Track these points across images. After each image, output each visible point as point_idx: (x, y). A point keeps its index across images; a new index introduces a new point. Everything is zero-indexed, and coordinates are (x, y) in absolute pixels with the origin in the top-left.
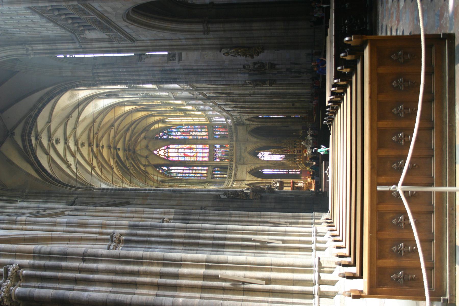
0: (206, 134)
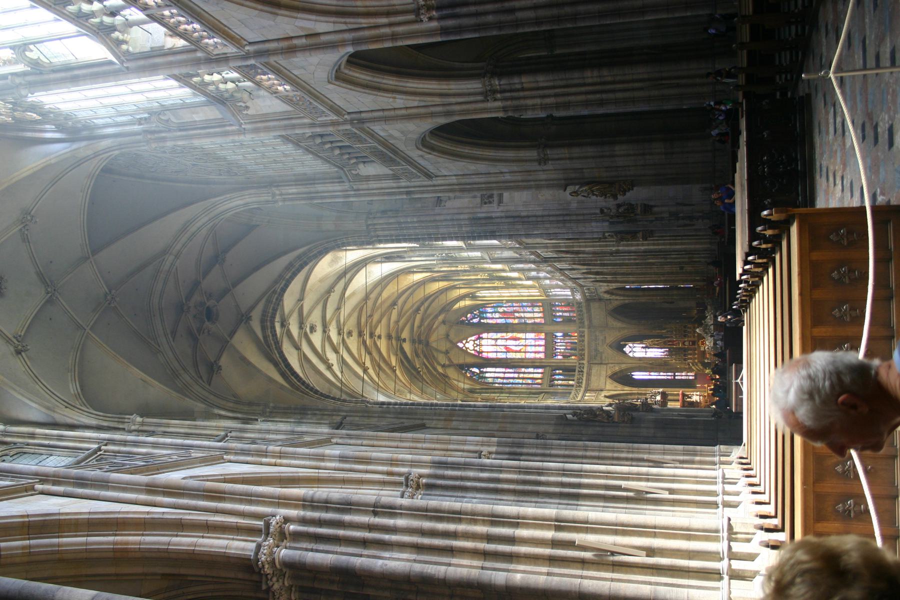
0: (541, 315)
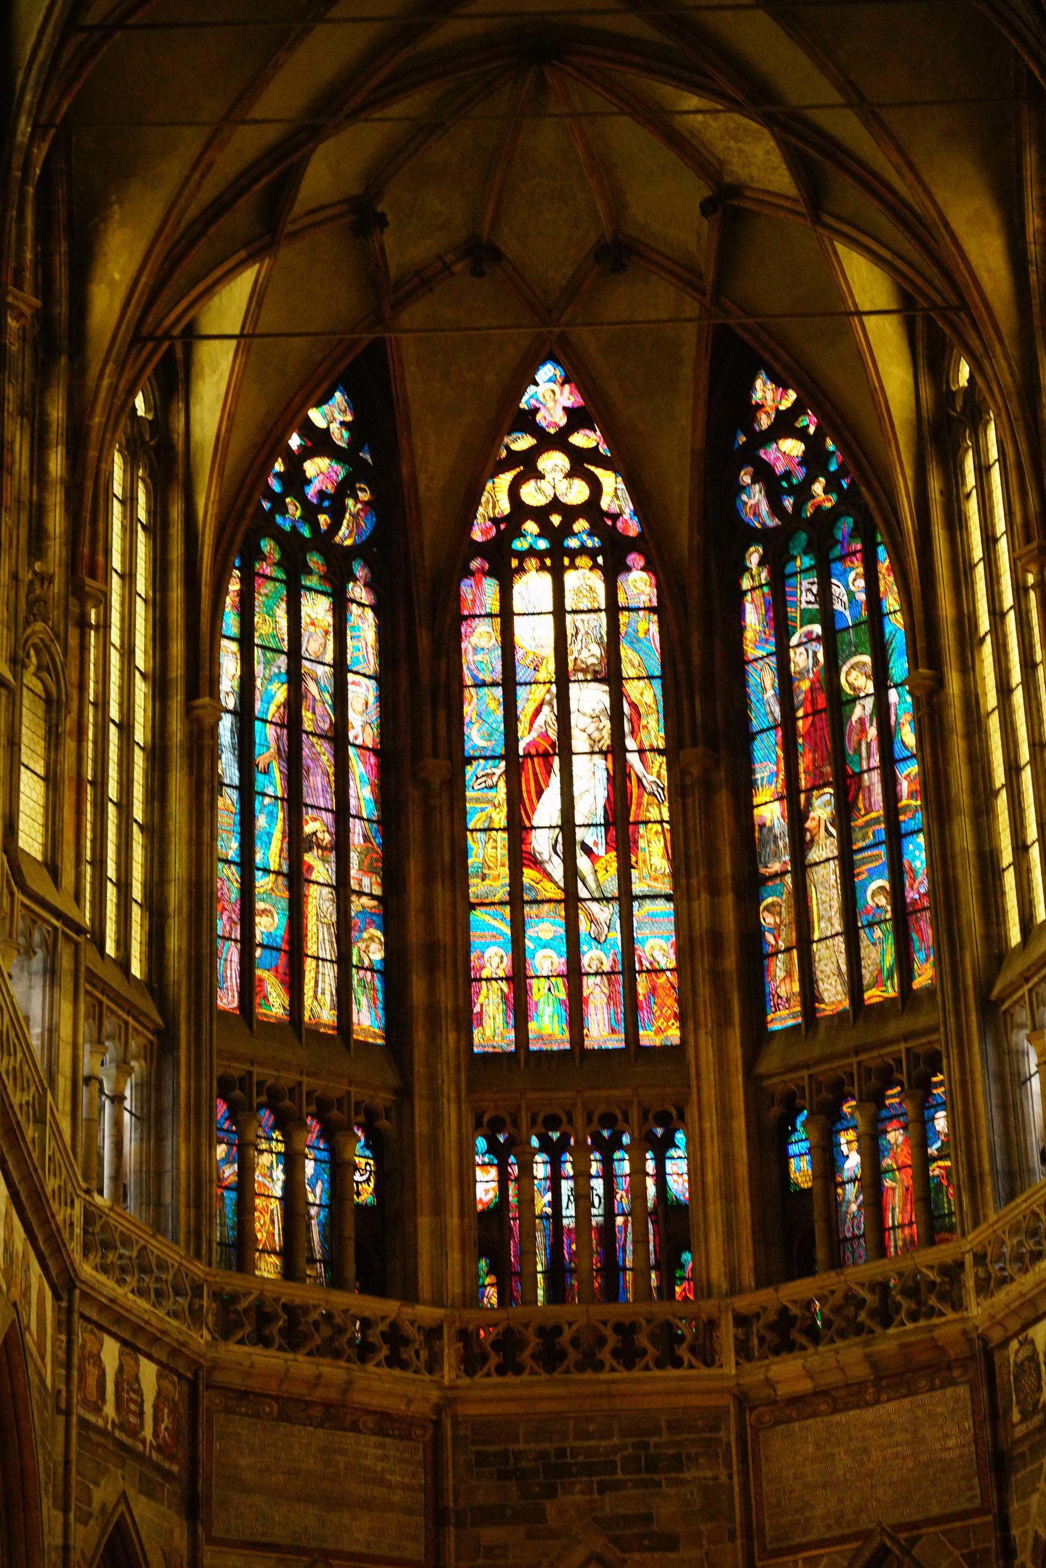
0: (833, 994)
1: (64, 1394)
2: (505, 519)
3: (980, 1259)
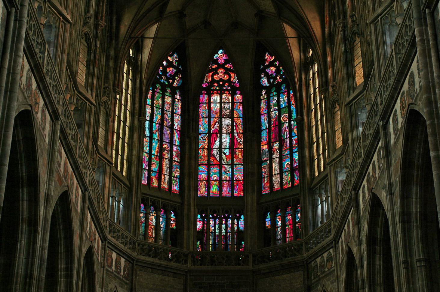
0: (277, 186)
1: (103, 263)
2: (210, 82)
3: (306, 243)
